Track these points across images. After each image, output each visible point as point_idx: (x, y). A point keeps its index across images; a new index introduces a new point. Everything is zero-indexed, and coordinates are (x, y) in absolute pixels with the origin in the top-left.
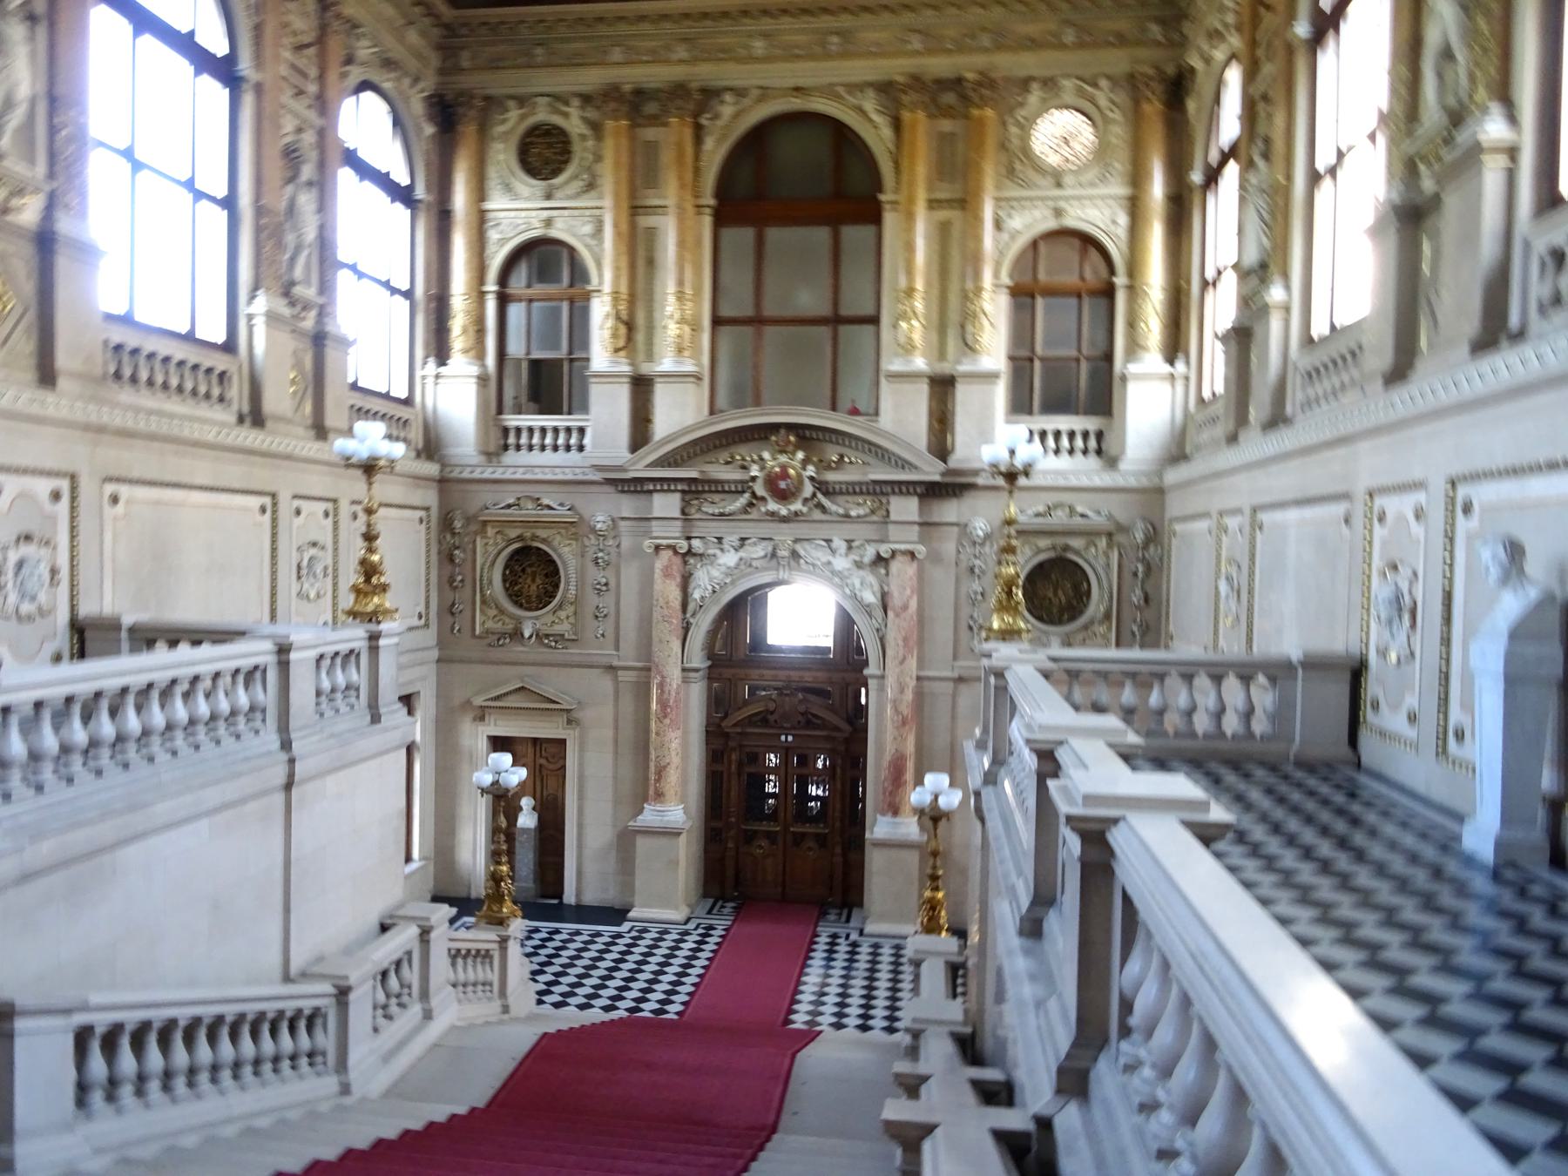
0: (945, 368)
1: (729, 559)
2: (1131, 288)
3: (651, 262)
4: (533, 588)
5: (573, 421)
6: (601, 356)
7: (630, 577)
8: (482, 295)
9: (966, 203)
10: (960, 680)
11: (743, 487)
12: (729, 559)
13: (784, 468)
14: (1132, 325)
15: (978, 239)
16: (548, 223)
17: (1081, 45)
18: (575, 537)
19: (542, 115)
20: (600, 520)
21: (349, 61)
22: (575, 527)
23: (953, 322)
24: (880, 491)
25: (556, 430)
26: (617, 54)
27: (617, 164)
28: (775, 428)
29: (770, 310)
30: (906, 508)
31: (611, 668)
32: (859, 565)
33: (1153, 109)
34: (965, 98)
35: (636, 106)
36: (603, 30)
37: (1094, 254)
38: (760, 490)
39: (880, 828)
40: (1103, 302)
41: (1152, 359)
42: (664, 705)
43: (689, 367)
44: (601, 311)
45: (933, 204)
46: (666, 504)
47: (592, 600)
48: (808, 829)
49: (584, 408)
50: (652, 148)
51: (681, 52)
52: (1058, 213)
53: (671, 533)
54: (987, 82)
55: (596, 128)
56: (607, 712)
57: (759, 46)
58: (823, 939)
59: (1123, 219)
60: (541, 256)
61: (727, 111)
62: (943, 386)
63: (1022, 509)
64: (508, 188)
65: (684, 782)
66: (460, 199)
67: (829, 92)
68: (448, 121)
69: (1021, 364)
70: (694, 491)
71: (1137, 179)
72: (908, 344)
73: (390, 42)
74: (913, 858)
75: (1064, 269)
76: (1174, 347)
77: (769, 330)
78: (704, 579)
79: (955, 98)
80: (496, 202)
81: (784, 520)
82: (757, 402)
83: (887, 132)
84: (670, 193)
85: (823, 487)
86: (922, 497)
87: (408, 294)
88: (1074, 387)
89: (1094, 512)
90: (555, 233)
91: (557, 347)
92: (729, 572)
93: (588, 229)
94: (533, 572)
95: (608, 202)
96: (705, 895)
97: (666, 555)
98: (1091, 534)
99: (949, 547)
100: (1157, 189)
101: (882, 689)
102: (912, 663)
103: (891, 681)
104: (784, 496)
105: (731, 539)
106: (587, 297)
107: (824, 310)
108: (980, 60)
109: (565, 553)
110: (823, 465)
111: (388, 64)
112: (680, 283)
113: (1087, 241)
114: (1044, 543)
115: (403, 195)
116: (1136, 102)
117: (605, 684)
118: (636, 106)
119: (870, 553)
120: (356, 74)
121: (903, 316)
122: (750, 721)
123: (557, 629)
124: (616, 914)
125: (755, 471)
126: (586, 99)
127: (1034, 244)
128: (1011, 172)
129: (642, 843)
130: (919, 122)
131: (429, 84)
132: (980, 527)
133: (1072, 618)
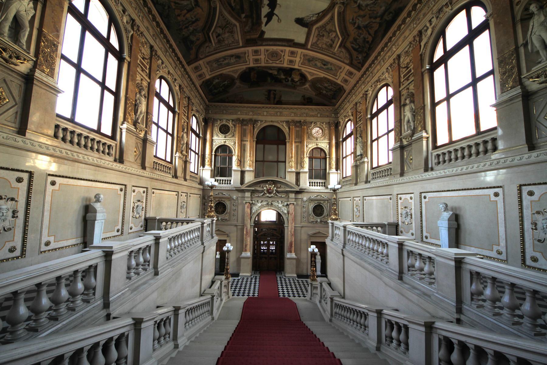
0: (298, 171)
1: (259, 205)
2: (329, 158)
3: (244, 150)
4: (221, 210)
5: (229, 178)
6: (235, 166)
7: (240, 208)
8: (212, 155)
9: (302, 142)
10: (302, 227)
11: (262, 191)
12: (259, 205)
13: (270, 188)
14: (330, 164)
15: (304, 149)
16: (225, 142)
17: (320, 117)
18: (230, 200)
19: (224, 122)
20: (235, 197)
21: (192, 110)
22: (230, 199)
23: (299, 163)
24: (287, 192)
25: (225, 180)
26: (239, 113)
27: (239, 132)
28: (269, 181)
29: (265, 160)
30: (292, 196)
31: (236, 226)
32: (283, 206)
33: (333, 128)
34: (301, 124)
35: (243, 122)
36: (237, 108)
37: (322, 152)
38: (266, 192)
39: (288, 255)
40: (324, 160)
41: (334, 170)
42: (247, 232)
43: (252, 169)
44: (235, 159)
45: (295, 142)
46: (248, 194)
47: (233, 212)
48: (272, 256)
49: (231, 176)
50: (245, 130)
51: (251, 113)
52: (317, 145)
53: (248, 200)
54: (305, 122)
55: (235, 126)
56: (235, 234)
57: (265, 113)
58: (278, 278)
59: (328, 146)
60: (223, 148)
61: (259, 124)
62: (298, 174)
63: (313, 196)
64: (217, 135)
65: (250, 247)
66: (208, 136)
67: (277, 122)
68: (207, 123)
69: (311, 170)
70: (253, 192)
71: (330, 140)
72: (291, 167)
73: (198, 107)
74: (295, 261)
75: (317, 154)
76: (337, 169)
77: (265, 163)
78: (255, 208)
79: (299, 124)
80: (215, 138)
81: (270, 197)
82: (263, 176)
83: (287, 129)
84: (249, 138)
85: (277, 191)
86: (295, 194)
87: (198, 154)
88: (320, 175)
89: (325, 197)
90: (226, 144)
91: (226, 165)
92: (259, 207)
93: (233, 143)
94: (221, 208)
95: (237, 139)
96: (253, 270)
97: (248, 204)
98: (324, 200)
99: (300, 203)
100: (334, 142)
101: (288, 229)
102: (293, 224)
103: (290, 228)
104: (270, 193)
105: (260, 201)
106: (232, 156)
107: (276, 160)
108: (304, 118)
109: (228, 203)
110: (277, 188)
111: (197, 111)
112: (250, 154)
113: (322, 150)
114: (316, 202)
115: (197, 135)
116: (330, 127)
117: (235, 228)
118: (243, 122)
119: (286, 204)
120: (193, 113)
121: (291, 161)
122: (262, 235)
123: (226, 218)
124: (237, 275)
125: (265, 188)
126: (233, 120)
127: (313, 149)
128: (309, 138)
129: (242, 260)
130: (292, 127)
131: (203, 116)
132: (305, 199)
133: (321, 216)
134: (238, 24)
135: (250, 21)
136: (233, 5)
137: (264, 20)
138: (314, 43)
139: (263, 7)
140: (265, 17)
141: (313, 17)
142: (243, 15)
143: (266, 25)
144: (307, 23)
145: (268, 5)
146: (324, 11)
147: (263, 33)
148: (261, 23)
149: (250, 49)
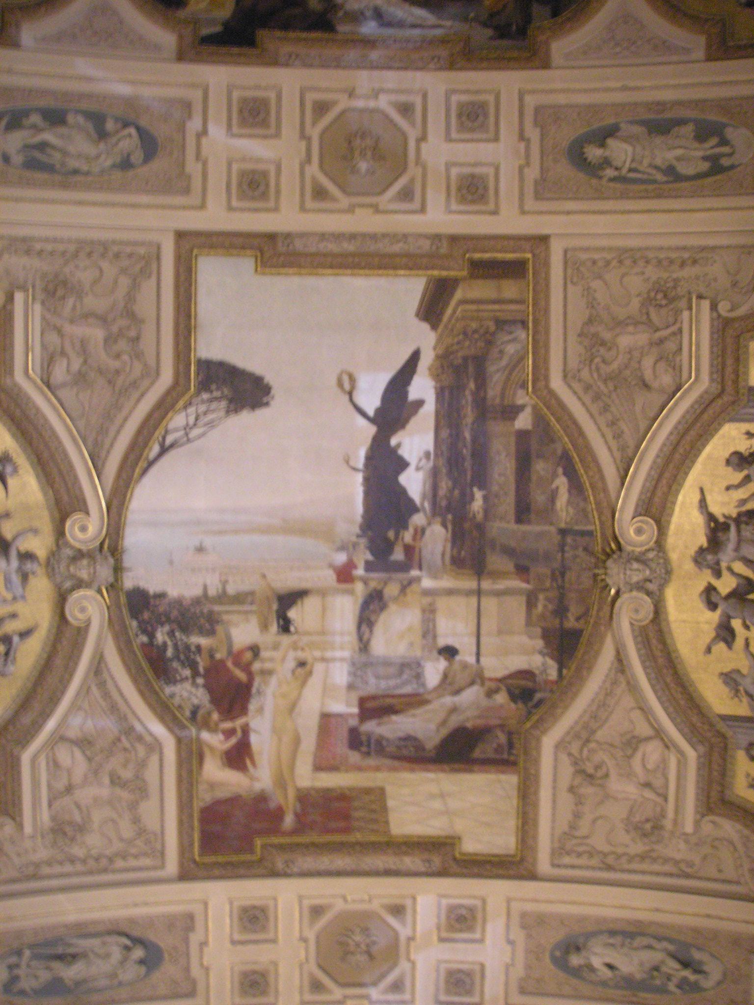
134: (556, 383)
135: (493, 392)
136: (561, 482)
137: (423, 388)
138: (145, 272)
139: (427, 455)
140: (420, 403)
141: (187, 428)
142: (524, 421)
143: (415, 357)
144: (204, 385)
145: (403, 465)
146: (145, 471)
147: (431, 310)
148: (436, 374)
149: (507, 220)
